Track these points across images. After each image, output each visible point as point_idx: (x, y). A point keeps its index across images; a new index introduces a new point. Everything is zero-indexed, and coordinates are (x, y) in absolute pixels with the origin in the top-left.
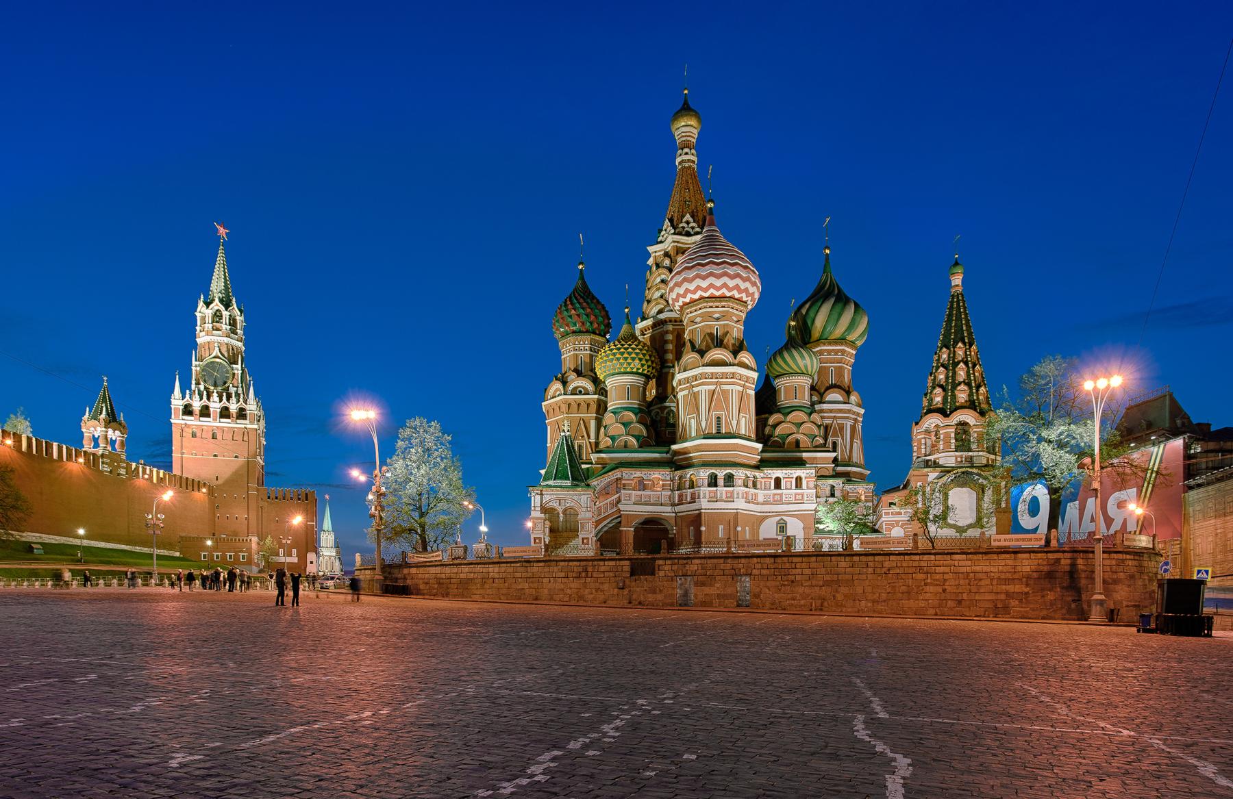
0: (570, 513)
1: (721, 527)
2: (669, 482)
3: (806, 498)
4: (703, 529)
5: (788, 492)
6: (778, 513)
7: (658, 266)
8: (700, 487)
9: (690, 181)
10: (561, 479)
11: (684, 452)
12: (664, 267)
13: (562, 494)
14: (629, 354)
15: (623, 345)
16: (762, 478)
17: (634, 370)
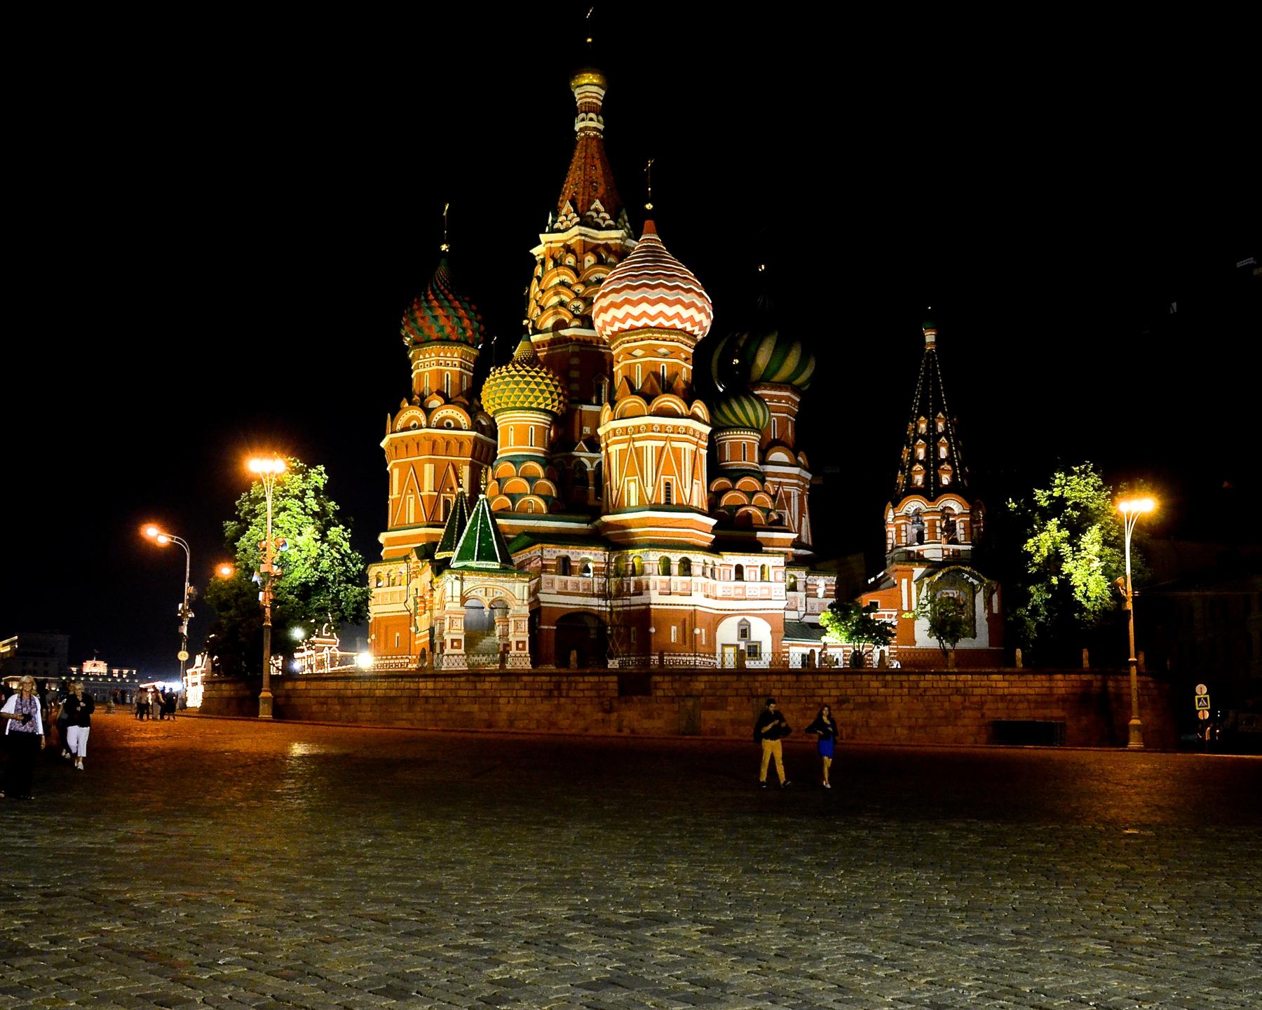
0: (502, 606)
1: (674, 628)
2: (603, 566)
3: (773, 594)
4: (653, 630)
5: (752, 586)
6: (739, 612)
7: (557, 264)
8: (649, 574)
10: (486, 559)
11: (622, 526)
12: (567, 266)
13: (490, 581)
14: (537, 384)
15: (528, 371)
16: (721, 565)
17: (542, 406)
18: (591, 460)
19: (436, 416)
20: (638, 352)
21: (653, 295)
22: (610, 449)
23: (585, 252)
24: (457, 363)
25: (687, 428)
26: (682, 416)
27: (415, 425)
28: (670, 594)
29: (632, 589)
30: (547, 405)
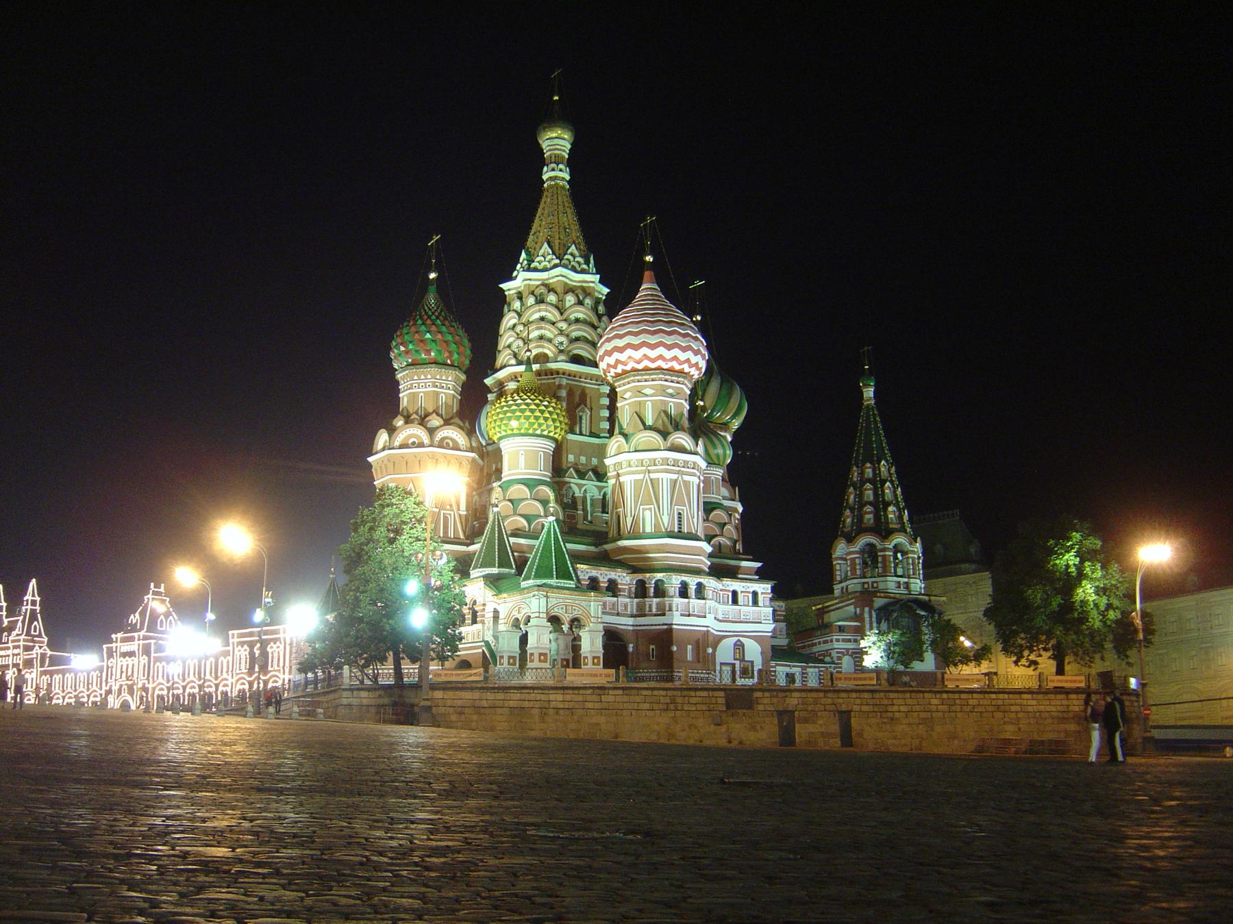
1: (689, 647)
4: (675, 648)
8: (672, 597)
9: (567, 205)
12: (550, 304)
16: (721, 590)
18: (580, 486)
19: (439, 436)
20: (648, 391)
21: (669, 340)
22: (622, 479)
23: (566, 293)
24: (450, 386)
25: (694, 463)
26: (691, 453)
27: (414, 443)
28: (689, 615)
29: (654, 610)
30: (555, 433)
